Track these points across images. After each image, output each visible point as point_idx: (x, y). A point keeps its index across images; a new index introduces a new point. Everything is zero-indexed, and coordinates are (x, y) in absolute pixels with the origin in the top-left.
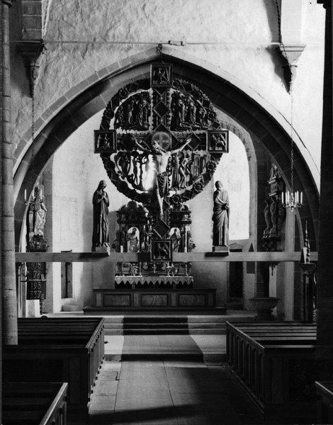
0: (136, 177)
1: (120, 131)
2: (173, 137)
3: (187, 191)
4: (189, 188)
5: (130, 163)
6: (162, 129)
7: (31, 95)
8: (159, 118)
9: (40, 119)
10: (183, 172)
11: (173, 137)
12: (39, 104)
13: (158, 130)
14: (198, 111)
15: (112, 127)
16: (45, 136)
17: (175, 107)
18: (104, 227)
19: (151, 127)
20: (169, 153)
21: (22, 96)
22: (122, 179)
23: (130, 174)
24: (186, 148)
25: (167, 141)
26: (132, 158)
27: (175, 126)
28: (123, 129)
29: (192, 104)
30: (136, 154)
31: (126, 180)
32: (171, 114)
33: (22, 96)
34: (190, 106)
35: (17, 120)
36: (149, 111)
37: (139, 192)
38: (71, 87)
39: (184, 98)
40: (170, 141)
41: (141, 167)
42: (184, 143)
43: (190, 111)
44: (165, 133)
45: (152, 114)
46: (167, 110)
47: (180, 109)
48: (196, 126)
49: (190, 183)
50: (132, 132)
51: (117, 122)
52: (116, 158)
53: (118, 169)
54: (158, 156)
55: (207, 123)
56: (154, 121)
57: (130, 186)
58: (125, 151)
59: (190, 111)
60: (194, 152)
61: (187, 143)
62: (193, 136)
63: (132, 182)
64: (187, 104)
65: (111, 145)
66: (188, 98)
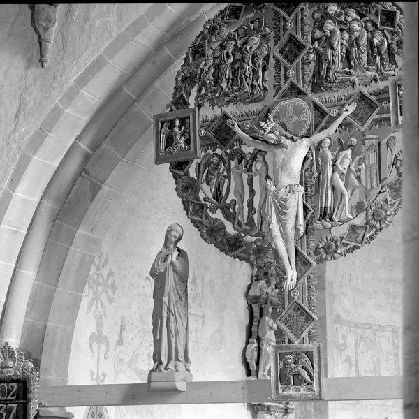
0: (241, 209)
2: (316, 107)
3: (354, 228)
4: (359, 221)
5: (228, 177)
6: (295, 91)
7: (42, 61)
8: (286, 69)
9: (56, 107)
10: (341, 184)
11: (316, 107)
12: (55, 78)
13: (284, 96)
14: (370, 42)
15: (192, 101)
16: (84, 146)
18: (172, 325)
19: (271, 92)
20: (306, 142)
21: (28, 67)
22: (213, 216)
23: (228, 201)
25: (303, 118)
26: (233, 163)
27: (319, 83)
28: (213, 105)
29: (356, 26)
30: (241, 157)
31: (219, 215)
32: (312, 57)
33: (28, 67)
34: (350, 31)
35: (17, 116)
36: (267, 59)
37: (249, 238)
38: (114, 34)
39: (339, 15)
40: (309, 116)
41: (250, 183)
42: (339, 115)
44: (299, 101)
45: (272, 61)
46: (301, 47)
47: (328, 41)
48: (368, 73)
50: (230, 110)
51: (203, 91)
52: (198, 170)
53: (206, 192)
54: (278, 151)
55: (392, 60)
56: (277, 77)
57: (230, 229)
58: (219, 151)
61: (345, 114)
62: (362, 97)
63: (230, 216)
64: (345, 27)
65: (187, 142)
66: (346, 14)
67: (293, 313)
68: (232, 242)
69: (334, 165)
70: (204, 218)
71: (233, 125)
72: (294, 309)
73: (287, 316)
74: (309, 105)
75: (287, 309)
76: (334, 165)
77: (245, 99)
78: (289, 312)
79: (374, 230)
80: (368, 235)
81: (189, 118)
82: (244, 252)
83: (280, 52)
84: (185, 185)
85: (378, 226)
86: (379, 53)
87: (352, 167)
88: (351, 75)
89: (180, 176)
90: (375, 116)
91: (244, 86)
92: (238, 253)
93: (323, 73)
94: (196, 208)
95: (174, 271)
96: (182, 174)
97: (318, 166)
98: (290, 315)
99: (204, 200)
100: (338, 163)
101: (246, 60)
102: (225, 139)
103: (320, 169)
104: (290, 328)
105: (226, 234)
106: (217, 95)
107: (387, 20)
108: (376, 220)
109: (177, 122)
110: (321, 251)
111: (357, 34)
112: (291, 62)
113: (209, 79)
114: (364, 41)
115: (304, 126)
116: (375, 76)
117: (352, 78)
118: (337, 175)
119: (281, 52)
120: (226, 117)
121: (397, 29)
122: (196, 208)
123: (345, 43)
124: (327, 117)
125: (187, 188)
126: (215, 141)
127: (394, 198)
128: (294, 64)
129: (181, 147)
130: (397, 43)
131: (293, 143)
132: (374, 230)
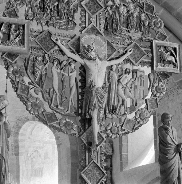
1: (35, 26)
2: (109, 44)
14: (139, 18)
17: (111, 7)
22: (34, 94)
24: (128, 61)
43: (130, 14)
44: (98, 37)
45: (79, 9)
49: (132, 109)
59: (130, 14)
60: (135, 68)
67: (92, 169)
68: (49, 116)
69: (119, 81)
70: (29, 96)
71: (57, 40)
72: (92, 167)
73: (87, 171)
74: (105, 41)
75: (88, 166)
76: (119, 81)
77: (62, 26)
78: (89, 168)
79: (139, 124)
80: (136, 127)
81: (23, 26)
82: (59, 124)
83: (85, 5)
84: (15, 70)
85: (141, 123)
86: (144, 25)
87: (128, 85)
88: (129, 32)
89: (11, 64)
90: (143, 59)
91: (63, 18)
92: (54, 124)
93: (114, 26)
94: (23, 88)
95: (5, 129)
96: (13, 62)
97: (109, 80)
98: (90, 171)
99: (29, 83)
100: (121, 80)
101: (65, 2)
102: (48, 47)
103: (110, 81)
104: (89, 179)
105: (45, 110)
106: (44, 17)
107: (149, 9)
108: (141, 119)
109: (13, 26)
110: (109, 131)
111: (132, 11)
112: (93, 14)
113: (37, 6)
114: (135, 16)
115: (102, 54)
116: (142, 38)
117: (130, 34)
118: (120, 87)
119: (86, 5)
120: (50, 34)
121: (154, 15)
122: (23, 88)
123: (125, 13)
124: (116, 52)
125: (17, 72)
126: (40, 46)
127: (151, 108)
128: (95, 16)
129: (16, 43)
130: (154, 23)
131: (101, 62)
132: (139, 124)
